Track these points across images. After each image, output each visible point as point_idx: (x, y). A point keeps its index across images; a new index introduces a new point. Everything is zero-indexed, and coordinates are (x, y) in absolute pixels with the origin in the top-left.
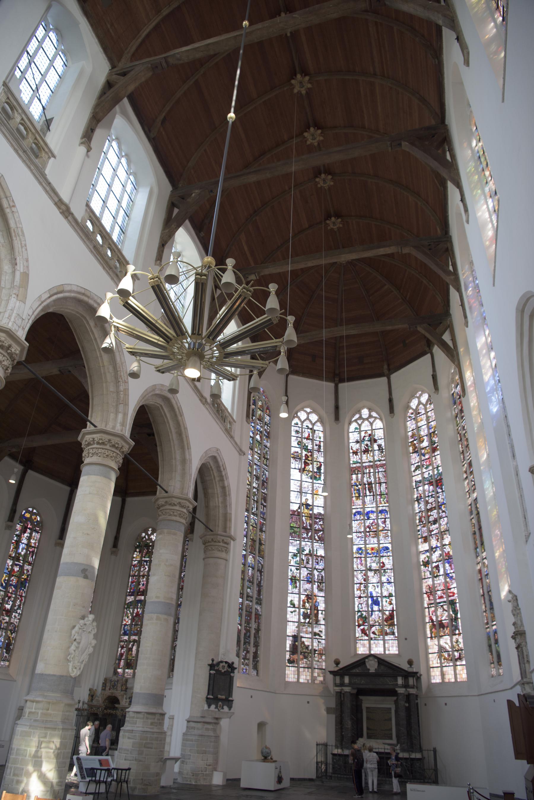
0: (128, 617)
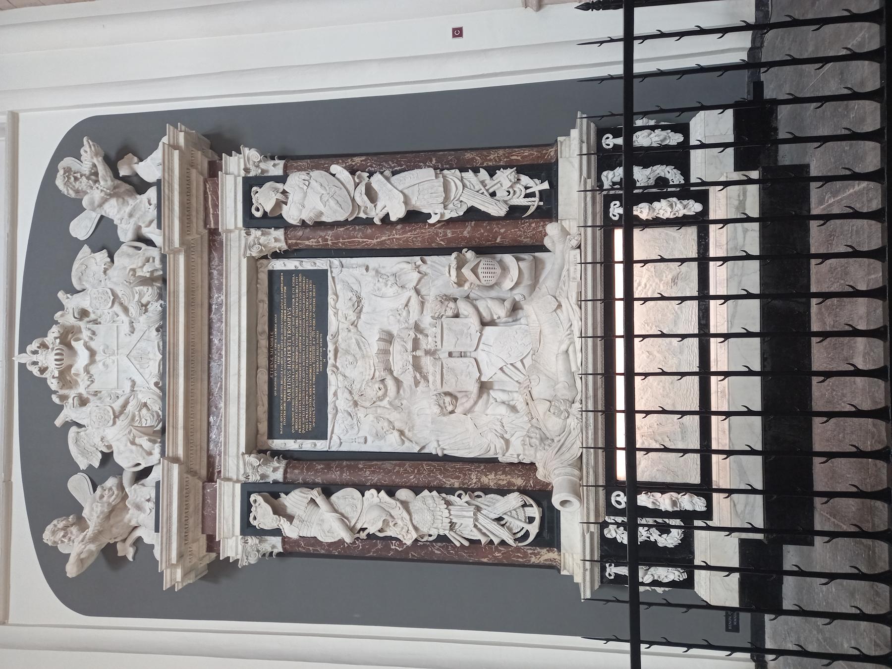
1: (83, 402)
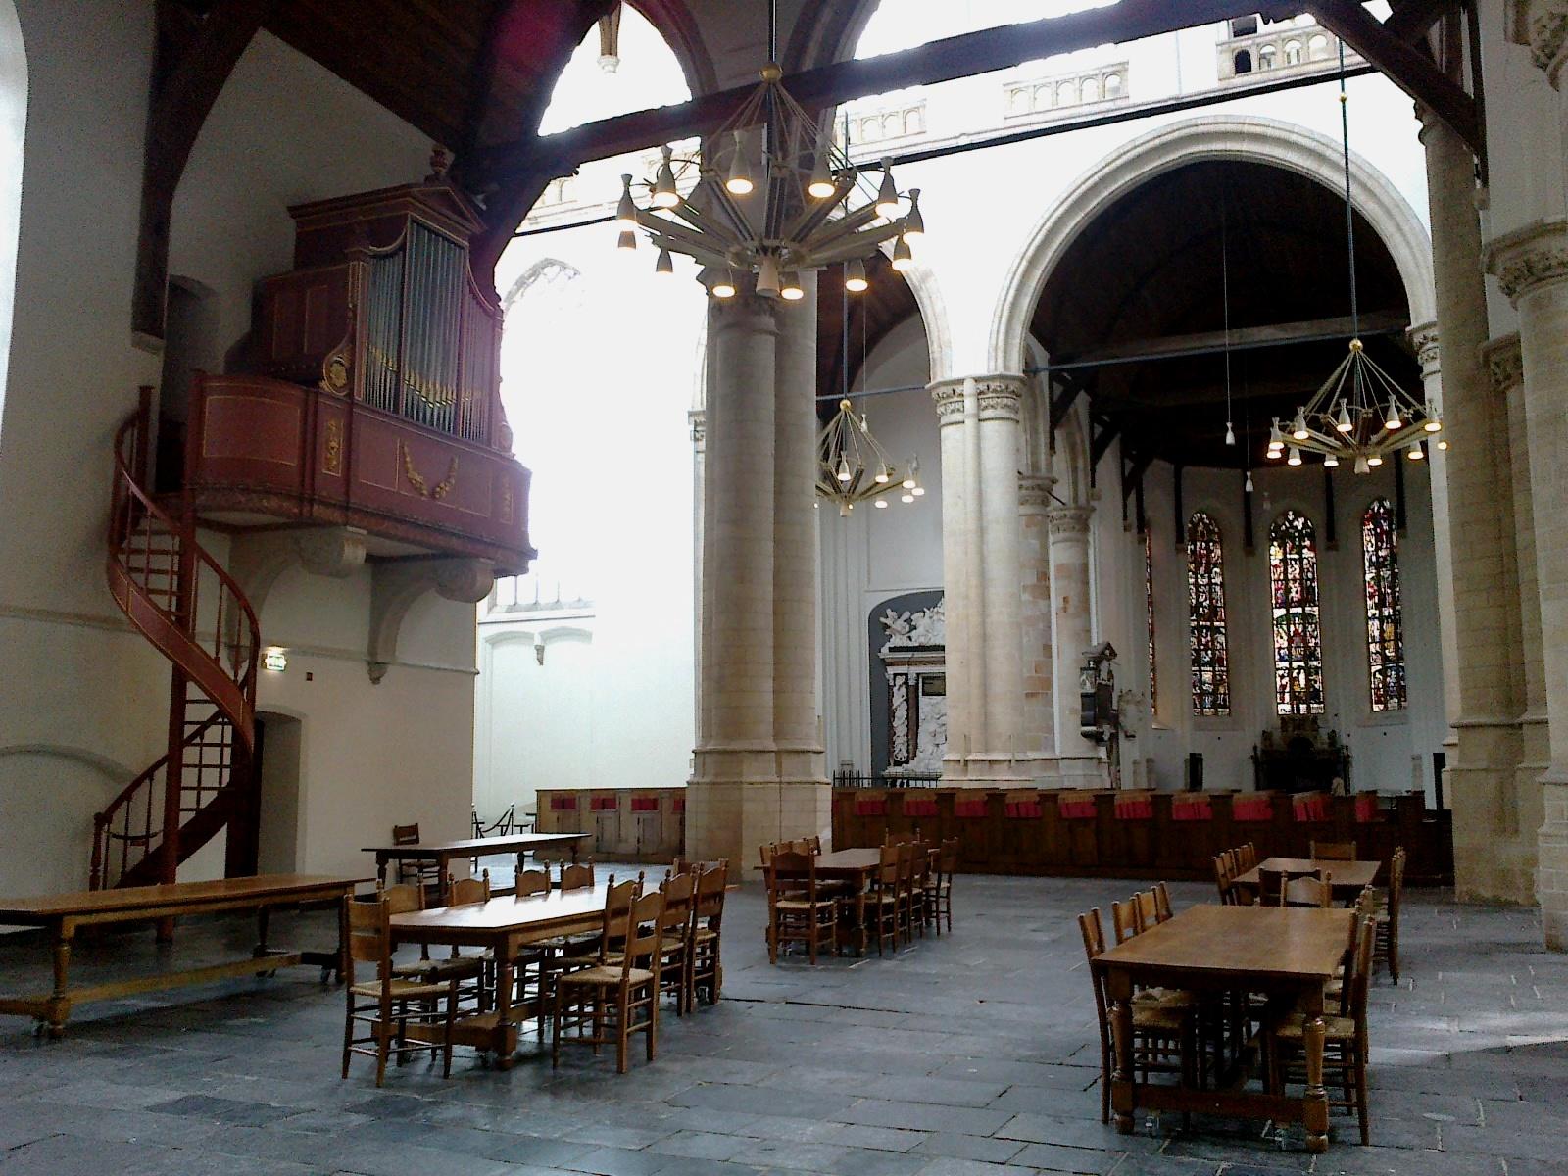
0: (1281, 638)
1: (931, 618)
